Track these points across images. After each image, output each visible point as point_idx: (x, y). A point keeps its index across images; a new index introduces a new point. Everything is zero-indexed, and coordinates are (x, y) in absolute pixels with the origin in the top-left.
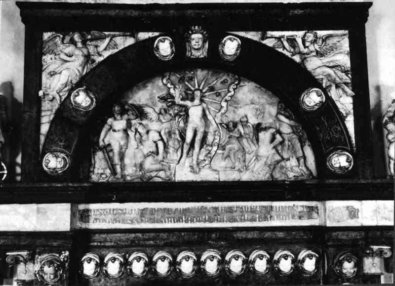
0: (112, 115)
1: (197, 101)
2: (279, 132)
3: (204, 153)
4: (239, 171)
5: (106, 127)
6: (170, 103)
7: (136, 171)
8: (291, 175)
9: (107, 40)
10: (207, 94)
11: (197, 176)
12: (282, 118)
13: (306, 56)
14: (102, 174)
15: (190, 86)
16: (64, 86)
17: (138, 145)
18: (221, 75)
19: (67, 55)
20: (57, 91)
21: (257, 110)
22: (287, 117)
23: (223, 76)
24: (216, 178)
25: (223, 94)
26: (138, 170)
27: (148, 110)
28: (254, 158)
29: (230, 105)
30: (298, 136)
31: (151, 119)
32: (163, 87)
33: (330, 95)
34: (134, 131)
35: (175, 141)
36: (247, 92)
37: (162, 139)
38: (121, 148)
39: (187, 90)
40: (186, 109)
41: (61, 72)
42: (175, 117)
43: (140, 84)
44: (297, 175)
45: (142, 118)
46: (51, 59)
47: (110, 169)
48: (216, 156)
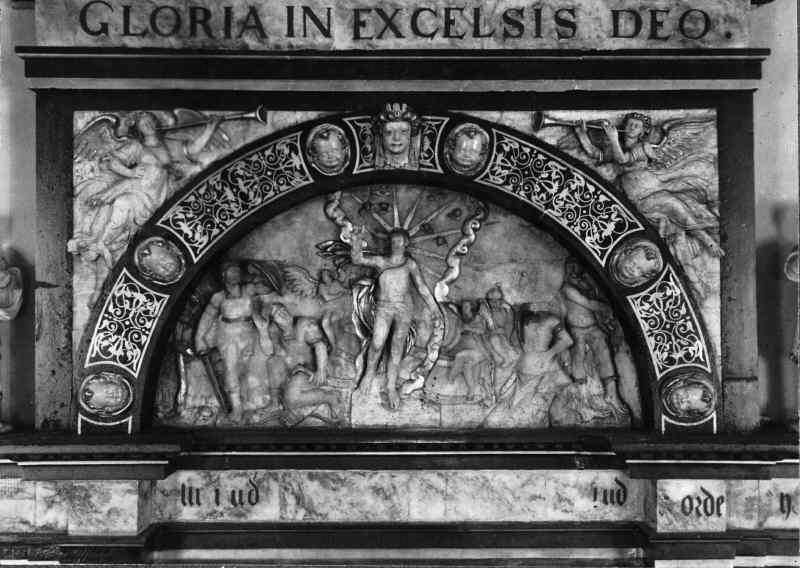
0: (221, 285)
1: (397, 258)
2: (568, 326)
3: (411, 366)
4: (481, 403)
5: (211, 311)
6: (342, 260)
7: (271, 402)
8: (589, 415)
9: (208, 133)
10: (418, 240)
11: (396, 414)
12: (574, 294)
13: (627, 169)
14: (201, 408)
15: (382, 222)
16: (120, 230)
17: (275, 349)
18: (446, 201)
19: (125, 165)
20: (104, 242)
21: (522, 275)
22: (582, 292)
23: (452, 201)
24: (435, 420)
25: (451, 241)
26: (276, 400)
27: (295, 273)
28: (514, 377)
29: (466, 264)
30: (604, 331)
31: (302, 292)
32: (328, 224)
33: (672, 252)
34: (267, 318)
35: (350, 340)
37: (324, 338)
38: (242, 353)
39: (377, 231)
40: (374, 274)
41: (113, 201)
42: (351, 288)
43: (279, 218)
44: (600, 415)
45: (284, 289)
46: (92, 170)
47: (219, 398)
48: (435, 369)
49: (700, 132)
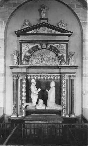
27: (37, 55)
36: (51, 53)
49: (65, 45)
